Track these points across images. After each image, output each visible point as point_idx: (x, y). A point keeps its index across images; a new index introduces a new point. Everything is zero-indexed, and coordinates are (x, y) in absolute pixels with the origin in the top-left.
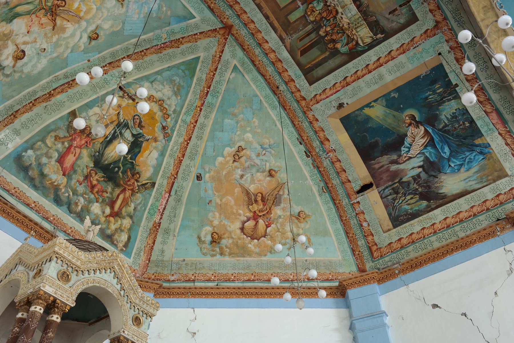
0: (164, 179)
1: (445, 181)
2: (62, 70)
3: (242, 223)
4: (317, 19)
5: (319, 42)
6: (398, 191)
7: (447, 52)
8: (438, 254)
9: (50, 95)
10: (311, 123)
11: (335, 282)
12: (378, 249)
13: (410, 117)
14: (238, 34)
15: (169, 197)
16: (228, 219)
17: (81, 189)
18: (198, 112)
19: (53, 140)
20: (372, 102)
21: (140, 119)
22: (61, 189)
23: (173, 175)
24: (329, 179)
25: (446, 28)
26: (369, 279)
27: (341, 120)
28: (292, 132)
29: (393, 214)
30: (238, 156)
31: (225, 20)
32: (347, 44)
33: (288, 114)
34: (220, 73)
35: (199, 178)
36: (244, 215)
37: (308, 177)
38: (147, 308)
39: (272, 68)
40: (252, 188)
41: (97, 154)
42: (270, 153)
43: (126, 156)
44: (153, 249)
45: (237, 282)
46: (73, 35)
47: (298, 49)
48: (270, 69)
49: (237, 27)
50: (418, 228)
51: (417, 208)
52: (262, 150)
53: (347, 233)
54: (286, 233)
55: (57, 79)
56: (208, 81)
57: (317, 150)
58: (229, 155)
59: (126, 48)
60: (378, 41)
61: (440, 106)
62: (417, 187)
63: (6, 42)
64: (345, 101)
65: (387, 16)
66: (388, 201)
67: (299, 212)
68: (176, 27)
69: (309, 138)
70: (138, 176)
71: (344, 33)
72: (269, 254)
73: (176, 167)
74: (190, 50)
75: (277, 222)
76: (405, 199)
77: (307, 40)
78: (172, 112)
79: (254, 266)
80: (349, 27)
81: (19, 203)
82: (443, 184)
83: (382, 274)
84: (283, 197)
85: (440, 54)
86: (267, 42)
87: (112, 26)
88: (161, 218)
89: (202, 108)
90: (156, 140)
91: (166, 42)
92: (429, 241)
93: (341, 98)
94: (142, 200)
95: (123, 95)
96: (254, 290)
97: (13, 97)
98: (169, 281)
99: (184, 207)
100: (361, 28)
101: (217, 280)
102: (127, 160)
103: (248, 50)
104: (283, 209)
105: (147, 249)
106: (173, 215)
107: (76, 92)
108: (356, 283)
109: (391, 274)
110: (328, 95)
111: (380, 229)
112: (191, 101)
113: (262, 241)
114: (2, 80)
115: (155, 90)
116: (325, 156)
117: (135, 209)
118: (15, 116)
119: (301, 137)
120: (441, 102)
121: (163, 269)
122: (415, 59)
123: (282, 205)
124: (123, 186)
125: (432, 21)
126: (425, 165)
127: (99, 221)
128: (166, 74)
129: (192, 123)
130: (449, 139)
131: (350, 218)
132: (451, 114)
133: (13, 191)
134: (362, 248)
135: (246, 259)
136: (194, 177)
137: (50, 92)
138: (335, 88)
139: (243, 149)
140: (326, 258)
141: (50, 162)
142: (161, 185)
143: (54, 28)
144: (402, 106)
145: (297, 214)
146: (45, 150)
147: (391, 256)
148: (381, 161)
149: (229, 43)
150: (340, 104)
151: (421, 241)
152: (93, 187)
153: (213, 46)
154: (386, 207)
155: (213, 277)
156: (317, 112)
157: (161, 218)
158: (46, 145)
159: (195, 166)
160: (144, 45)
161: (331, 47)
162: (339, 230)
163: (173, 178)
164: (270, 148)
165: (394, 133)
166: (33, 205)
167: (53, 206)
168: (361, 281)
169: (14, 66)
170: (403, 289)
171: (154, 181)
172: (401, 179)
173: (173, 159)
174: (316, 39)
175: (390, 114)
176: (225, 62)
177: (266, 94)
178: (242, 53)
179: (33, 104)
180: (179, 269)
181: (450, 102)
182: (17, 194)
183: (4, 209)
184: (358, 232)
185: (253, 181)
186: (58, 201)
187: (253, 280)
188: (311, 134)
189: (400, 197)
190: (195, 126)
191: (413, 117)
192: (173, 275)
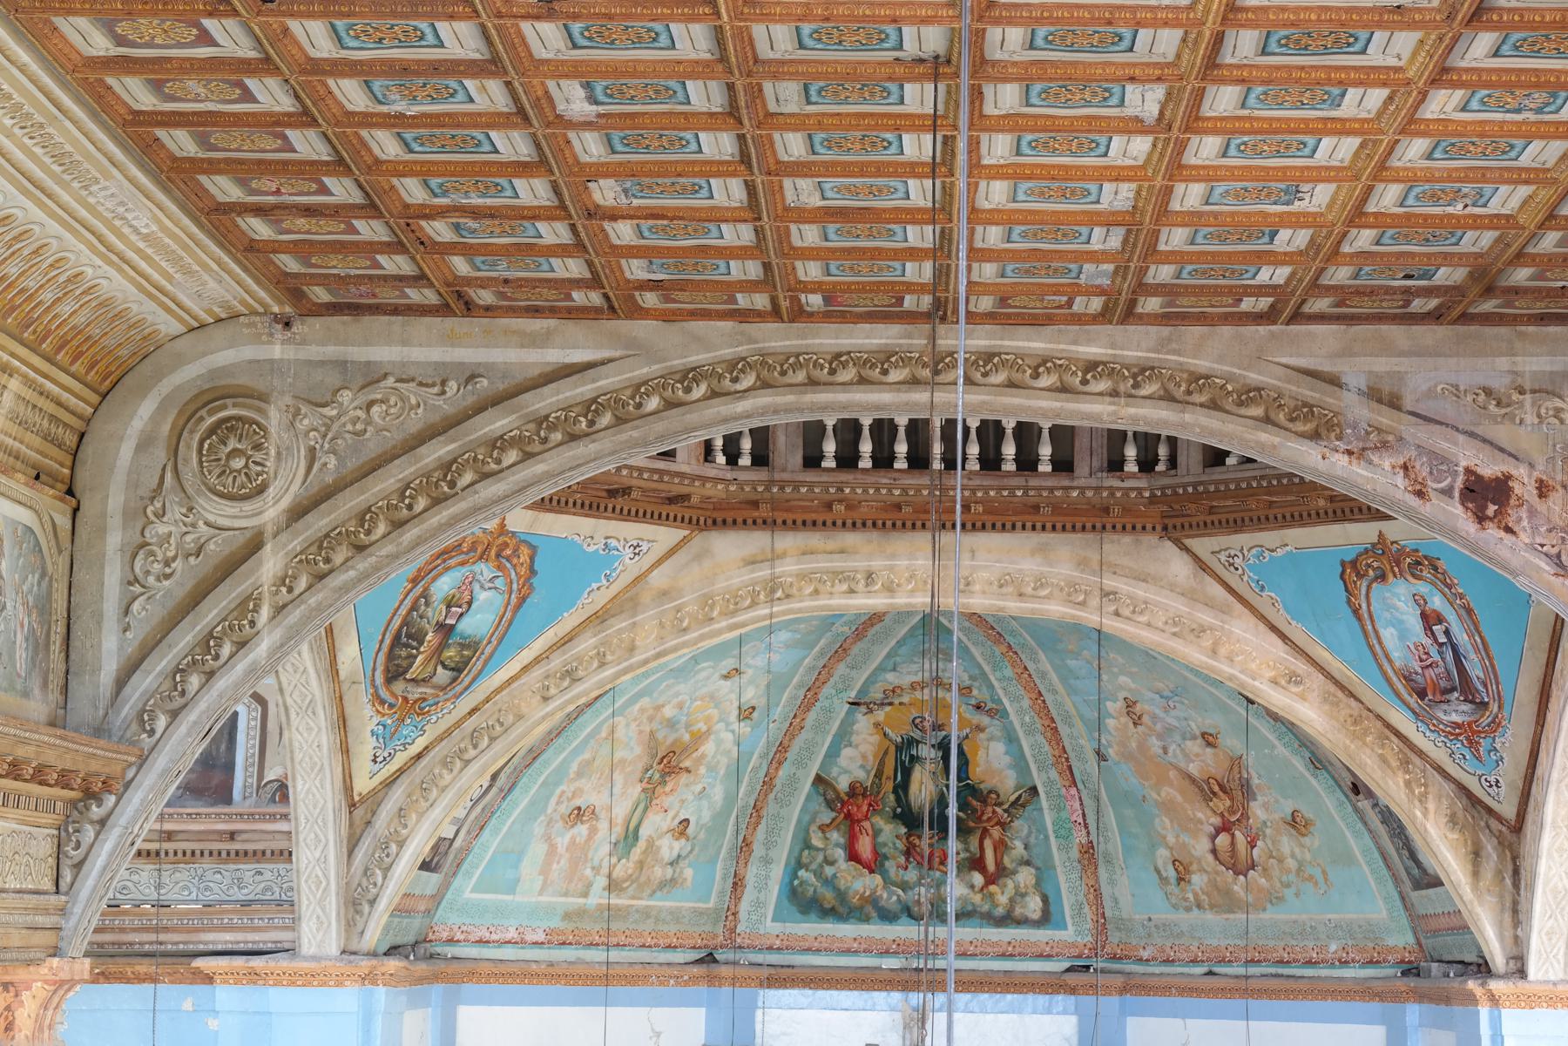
0: (1047, 772)
19: (820, 834)
22: (881, 896)
37: (1276, 742)
41: (899, 810)
70: (993, 796)
72: (1269, 906)
75: (1265, 836)
88: (1088, 833)
90: (980, 729)
105: (1091, 896)
124: (975, 828)
128: (903, 650)
142: (1049, 783)
146: (820, 858)
158: (818, 849)
171: (1031, 785)
186: (887, 916)
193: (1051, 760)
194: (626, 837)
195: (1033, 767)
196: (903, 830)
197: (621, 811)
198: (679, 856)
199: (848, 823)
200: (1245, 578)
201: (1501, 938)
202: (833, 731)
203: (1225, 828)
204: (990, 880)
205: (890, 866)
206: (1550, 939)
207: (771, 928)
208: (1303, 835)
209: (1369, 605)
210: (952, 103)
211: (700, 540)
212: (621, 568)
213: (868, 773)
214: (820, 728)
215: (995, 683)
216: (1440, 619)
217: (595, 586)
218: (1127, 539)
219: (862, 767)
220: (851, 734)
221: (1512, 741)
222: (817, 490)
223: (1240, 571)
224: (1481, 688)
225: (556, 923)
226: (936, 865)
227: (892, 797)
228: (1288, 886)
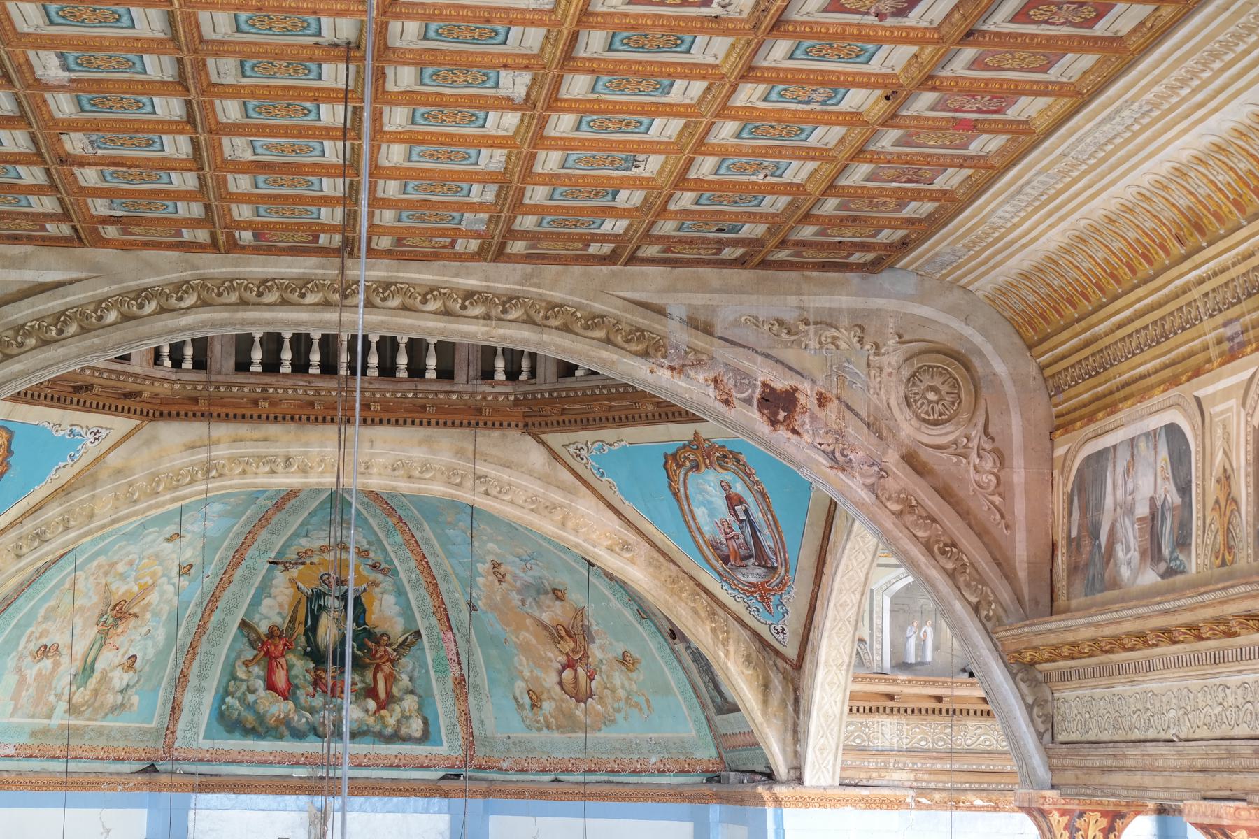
0: (429, 620)
19: (244, 668)
37: (611, 597)
41: (309, 649)
42: (538, 565)
70: (385, 638)
88: (461, 668)
90: (375, 584)
98: (501, 770)
117: (411, 679)
127: (367, 725)
128: (314, 520)
142: (430, 628)
146: (244, 687)
158: (242, 680)
171: (415, 629)
186: (298, 735)
193: (433, 610)
194: (84, 669)
196: (312, 665)
197: (80, 648)
198: (128, 685)
199: (267, 659)
200: (589, 466)
201: (784, 752)
202: (256, 585)
203: (570, 664)
204: (382, 706)
205: (301, 694)
206: (822, 753)
207: (202, 743)
208: (631, 671)
209: (686, 489)
210: (361, 80)
211: (149, 428)
212: (83, 450)
213: (284, 619)
214: (245, 582)
215: (389, 548)
216: (741, 501)
217: (61, 464)
218: (496, 434)
219: (279, 613)
220: (271, 587)
221: (795, 598)
222: (246, 390)
223: (585, 461)
224: (771, 555)
225: (25, 740)
226: (338, 694)
227: (303, 639)
228: (619, 711)
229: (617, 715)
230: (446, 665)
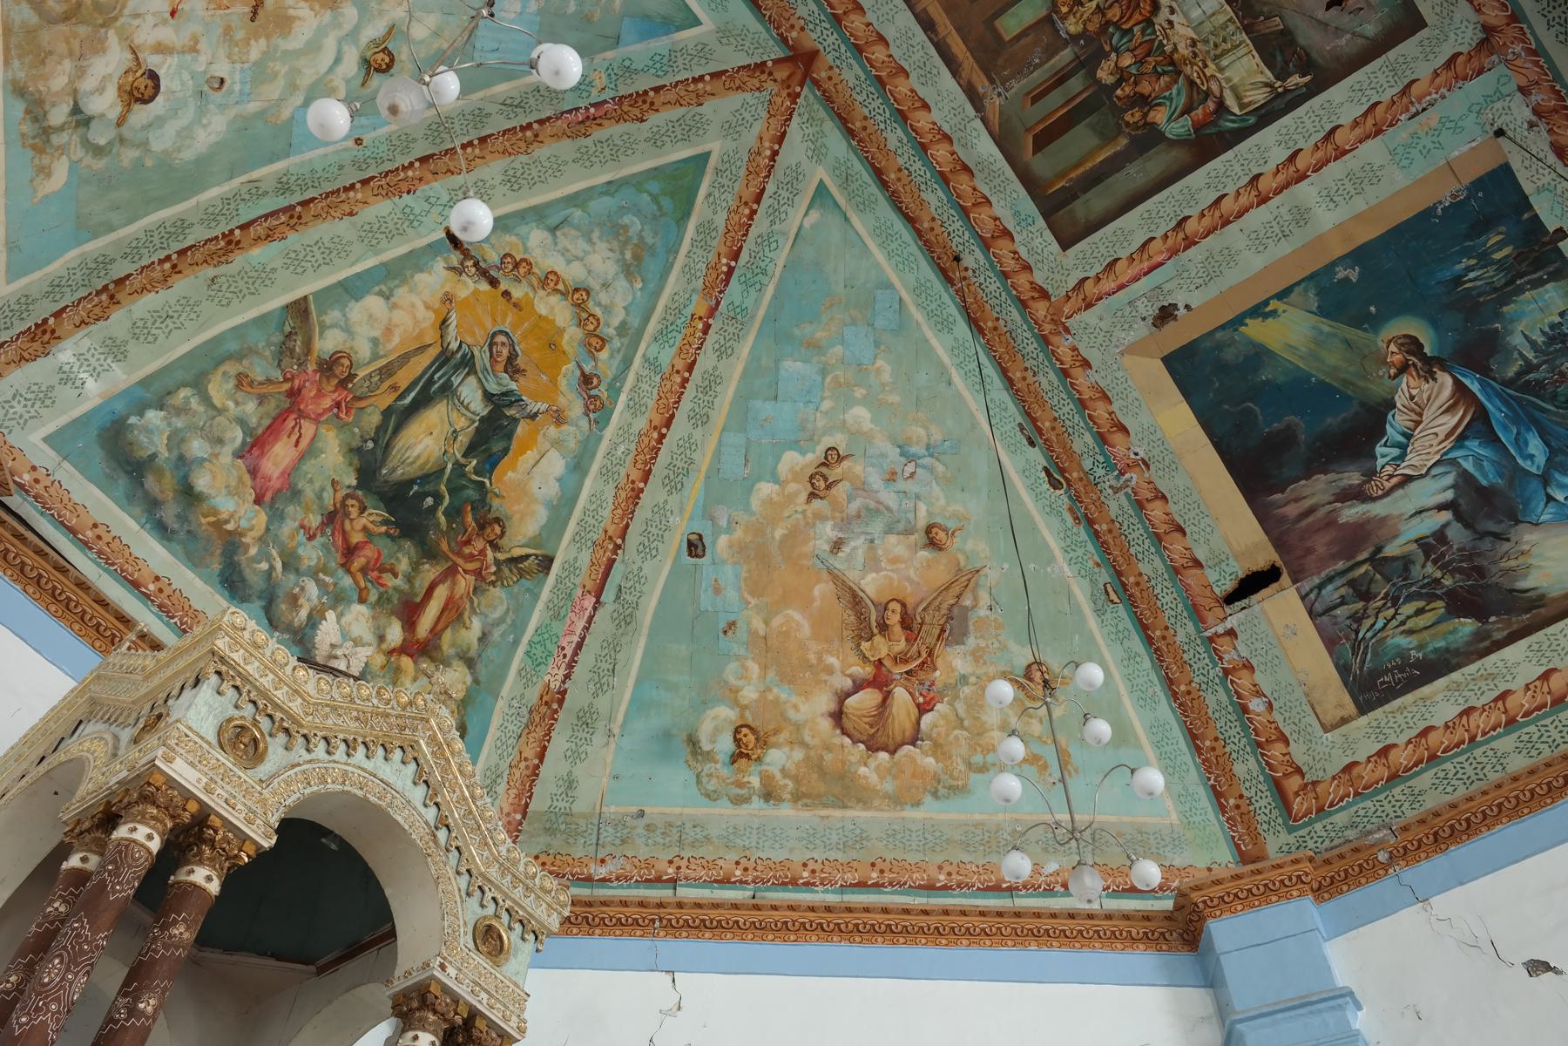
0: (580, 549)
1: (1535, 551)
2: (271, 161)
3: (835, 698)
4: (1091, 27)
5: (1097, 103)
6: (1369, 589)
7: (1526, 126)
8: (1532, 791)
9: (230, 243)
10: (1065, 373)
11: (1160, 898)
12: (1306, 785)
13: (1402, 345)
14: (834, 81)
15: (595, 609)
16: (790, 683)
17: (311, 554)
18: (699, 334)
19: (231, 384)
20: (1272, 298)
21: (512, 345)
22: (247, 547)
23: (610, 538)
24: (1128, 558)
25: (1518, 48)
26: (1282, 882)
27: (1168, 361)
28: (1003, 406)
29: (1355, 668)
30: (826, 479)
31: (794, 34)
32: (1187, 110)
33: (990, 348)
34: (771, 211)
35: (696, 548)
36: (843, 672)
37: (1058, 553)
38: (526, 903)
39: (940, 193)
40: (871, 585)
41: (370, 445)
42: (931, 470)
43: (463, 461)
44: (537, 775)
45: (820, 888)
46: (313, 47)
47: (1028, 130)
48: (934, 199)
49: (830, 58)
50: (1449, 711)
51: (1442, 644)
52: (903, 460)
53: (1193, 737)
54: (986, 731)
55: (256, 191)
56: (733, 234)
57: (1087, 464)
58: (796, 477)
59: (477, 112)
60: (1289, 97)
61: (1507, 304)
62: (1438, 574)
63: (103, 30)
64: (1180, 299)
65: (1321, 14)
66: (1335, 624)
67: (1029, 666)
68: (637, 51)
69: (1058, 425)
71: (1179, 73)
72: (928, 799)
73: (620, 511)
74: (678, 131)
75: (956, 697)
76: (1396, 613)
77: (1055, 98)
78: (616, 329)
79: (880, 839)
80: (1194, 53)
81: (105, 575)
82: (1530, 561)
83: (1328, 868)
84: (973, 617)
85: (1500, 133)
86: (926, 107)
87: (436, 34)
88: (567, 677)
89: (711, 321)
90: (559, 419)
91: (605, 102)
92: (1490, 753)
93: (1166, 287)
94: (508, 610)
95: (462, 264)
96: (880, 917)
97: (111, 229)
99: (642, 642)
100: (1234, 57)
101: (754, 882)
102: (464, 475)
103: (863, 135)
104: (973, 653)
105: (518, 774)
106: (605, 666)
107: (312, 243)
108: (1236, 895)
109: (1360, 866)
110: (1123, 279)
111: (1312, 720)
112: (676, 298)
113: (906, 756)
114: (81, 160)
115: (563, 255)
116: (1113, 483)
117: (483, 638)
118: (112, 297)
119: (1034, 421)
120: (1507, 292)
121: (571, 841)
122: (1415, 153)
123: (971, 642)
124: (447, 559)
125: (1471, 27)
126: (1461, 501)
129: (678, 372)
130: (1543, 410)
131: (1204, 687)
132: (1547, 329)
133: (89, 533)
134: (1247, 784)
135: (850, 813)
136: (680, 546)
137: (232, 231)
138: (1146, 258)
139: (840, 459)
140: (1126, 819)
141: (216, 456)
142: (571, 568)
143: (255, 13)
144: (1372, 309)
145: (1021, 672)
147: (1355, 808)
148: (1306, 492)
149: (802, 110)
150: (1163, 308)
151: (1463, 752)
152: (350, 552)
153: (751, 120)
154: (1330, 643)
155: (738, 873)
156: (1085, 337)
157: (567, 677)
158: (206, 400)
159: (682, 510)
160: (534, 107)
161: (1136, 119)
162: (1167, 727)
163: (611, 547)
164: (931, 455)
165: (1349, 399)
166: (152, 587)
167: (218, 597)
168: (1255, 891)
169: (121, 121)
170: (1409, 918)
172: (1379, 549)
173: (612, 485)
174: (1084, 95)
175: (1334, 335)
176: (788, 172)
177: (917, 280)
178: (844, 144)
179: (176, 263)
180: (623, 841)
181: (1540, 289)
182: (101, 545)
183: (54, 588)
184: (1232, 732)
185: (872, 563)
186: (233, 583)
187: (876, 885)
188: (1066, 409)
189: (1379, 610)
190: (686, 380)
191: (1412, 345)
192: (603, 861)
193: (597, 536)
195: (572, 526)
213: (375, 356)
214: (374, 235)
220: (404, 281)
227: (373, 419)
229: (974, 777)
230: (550, 654)
